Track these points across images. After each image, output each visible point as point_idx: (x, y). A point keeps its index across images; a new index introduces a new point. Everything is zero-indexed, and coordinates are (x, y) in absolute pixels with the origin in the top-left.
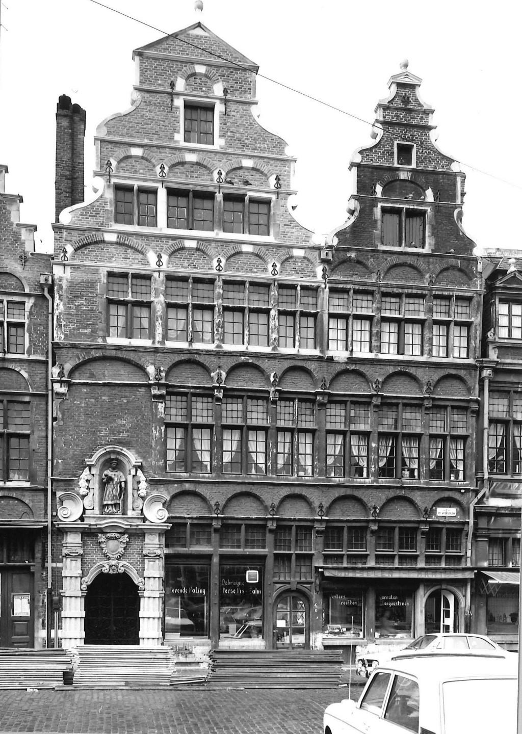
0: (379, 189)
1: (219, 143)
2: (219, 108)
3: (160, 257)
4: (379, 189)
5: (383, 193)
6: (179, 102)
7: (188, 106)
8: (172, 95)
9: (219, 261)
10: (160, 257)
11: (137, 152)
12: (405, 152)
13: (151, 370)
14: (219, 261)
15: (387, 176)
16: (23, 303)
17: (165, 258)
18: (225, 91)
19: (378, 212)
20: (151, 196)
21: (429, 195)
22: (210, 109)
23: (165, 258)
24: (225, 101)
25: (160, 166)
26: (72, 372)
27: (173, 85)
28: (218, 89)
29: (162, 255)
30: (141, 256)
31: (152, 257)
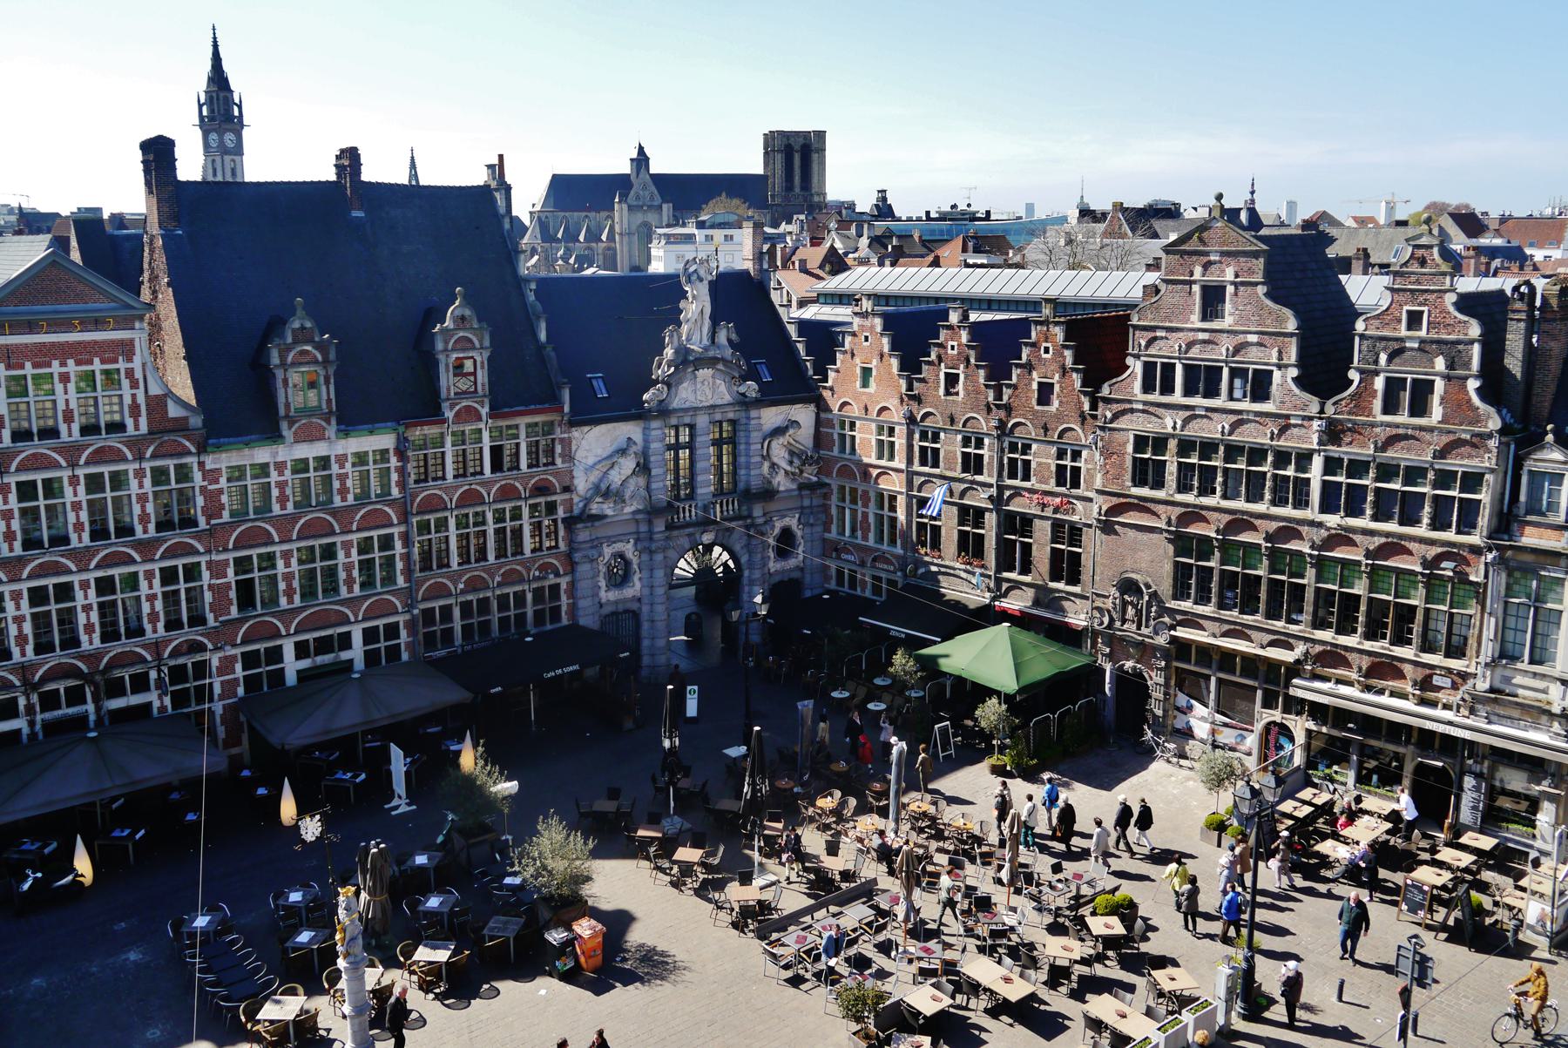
0: (1383, 358)
4: (1383, 358)
5: (1390, 360)
9: (1223, 427)
10: (1175, 423)
12: (1414, 320)
13: (1163, 517)
14: (1223, 427)
15: (1396, 346)
17: (1179, 423)
18: (1237, 276)
19: (1379, 383)
21: (1440, 364)
24: (1235, 284)
26: (1107, 512)
28: (1229, 275)
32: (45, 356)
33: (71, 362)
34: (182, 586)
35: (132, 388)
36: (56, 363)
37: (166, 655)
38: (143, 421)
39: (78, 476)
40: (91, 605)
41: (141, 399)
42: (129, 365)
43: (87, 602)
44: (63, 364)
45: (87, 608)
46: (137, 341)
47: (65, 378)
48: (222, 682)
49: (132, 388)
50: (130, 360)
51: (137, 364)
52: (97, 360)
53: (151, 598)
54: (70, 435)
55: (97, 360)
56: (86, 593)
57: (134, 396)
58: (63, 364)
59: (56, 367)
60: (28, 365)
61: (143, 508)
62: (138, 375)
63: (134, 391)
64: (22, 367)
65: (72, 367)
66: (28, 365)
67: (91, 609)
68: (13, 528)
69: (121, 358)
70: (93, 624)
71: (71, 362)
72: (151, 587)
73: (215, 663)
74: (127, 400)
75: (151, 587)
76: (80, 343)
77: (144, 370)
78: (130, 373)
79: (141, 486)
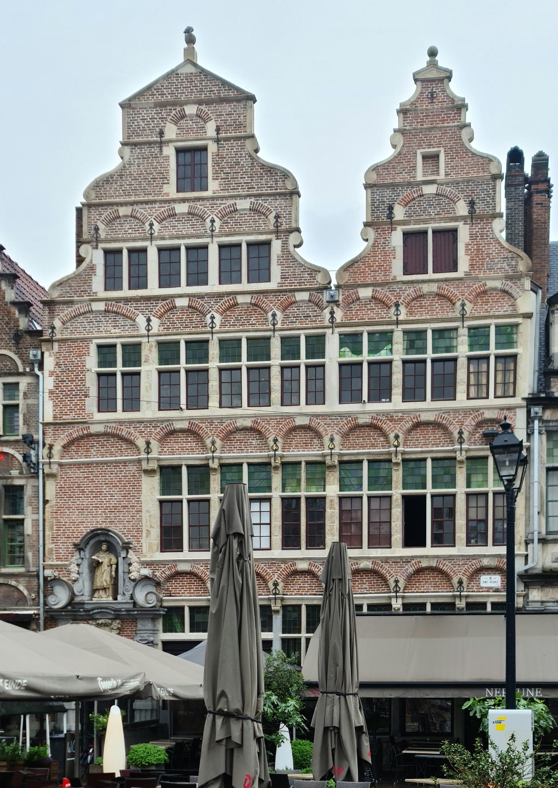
1: (213, 186)
2: (212, 148)
3: (149, 320)
6: (170, 151)
7: (179, 151)
8: (161, 144)
10: (149, 320)
11: (123, 211)
16: (17, 384)
17: (155, 322)
18: (218, 130)
20: (142, 255)
22: (204, 149)
23: (155, 322)
24: (217, 141)
25: (148, 222)
27: (161, 133)
29: (152, 318)
30: (129, 322)
31: (141, 320)
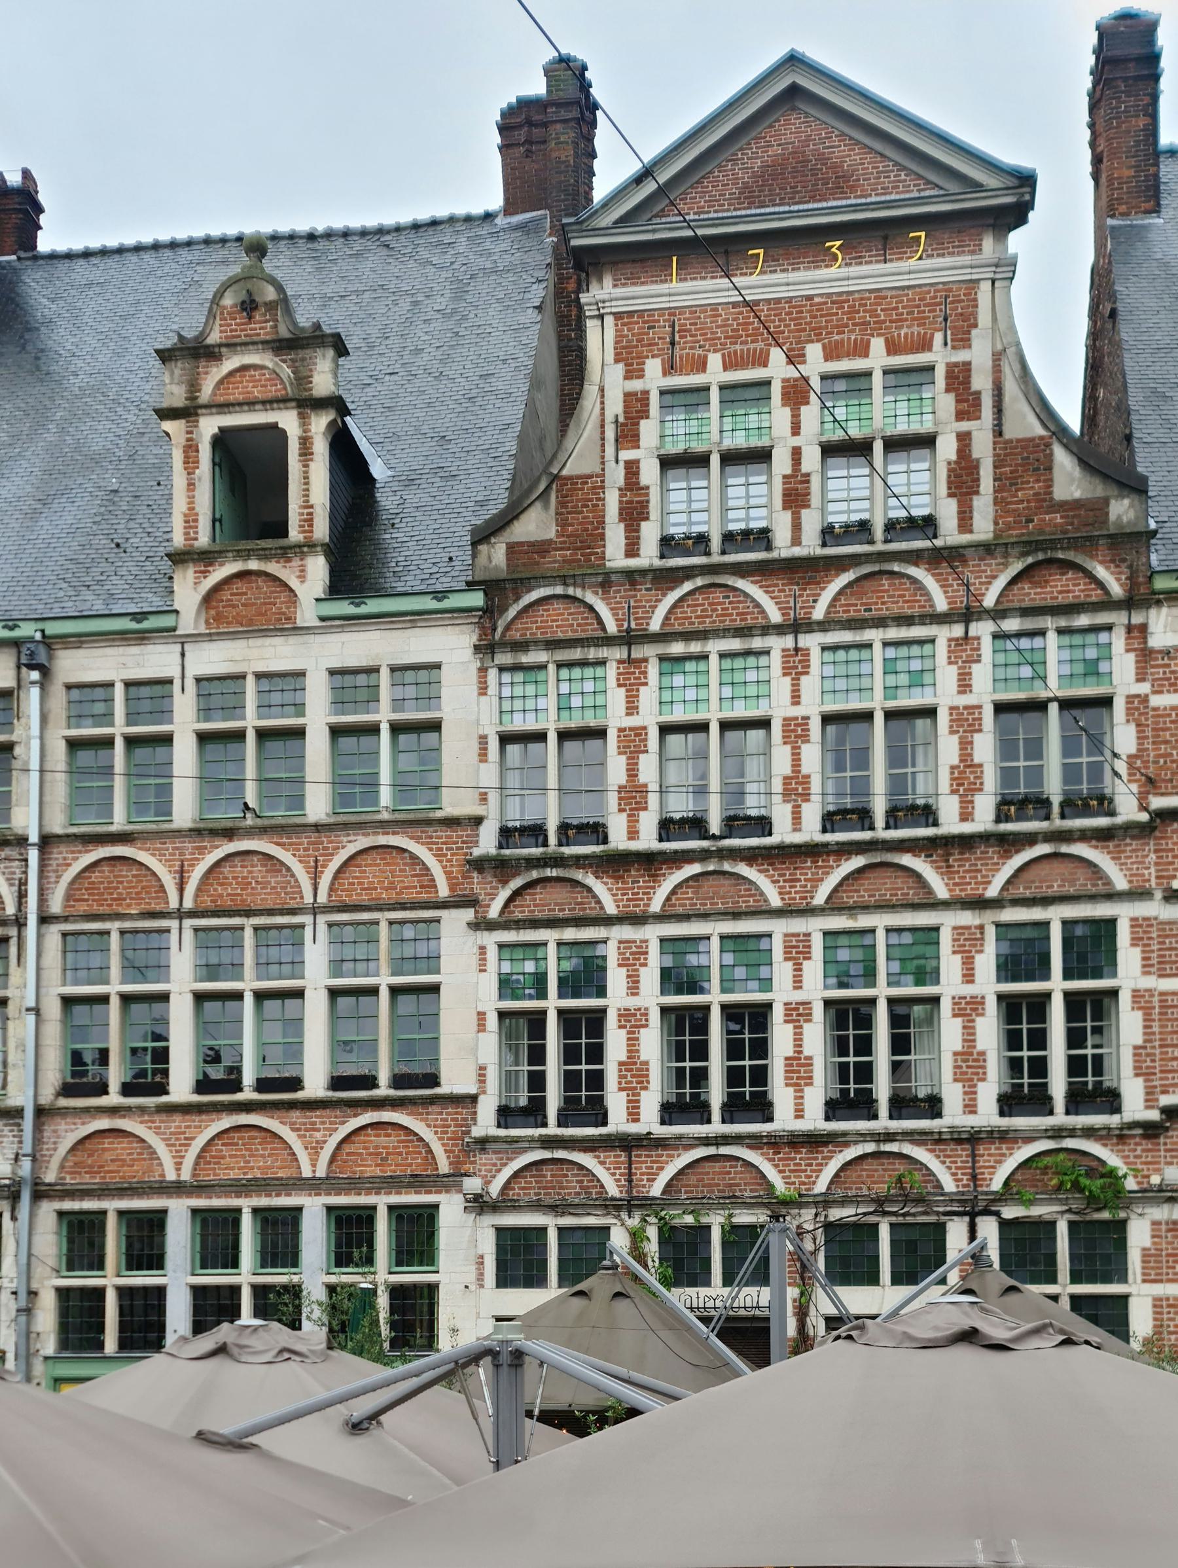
32: (755, 338)
33: (814, 351)
34: (1057, 984)
35: (960, 416)
36: (777, 356)
37: (997, 1185)
38: (983, 506)
39: (806, 652)
40: (807, 1004)
41: (983, 448)
42: (961, 356)
43: (798, 996)
44: (796, 358)
45: (798, 1013)
46: (985, 286)
47: (796, 394)
48: (1158, 1303)
49: (960, 416)
50: (962, 340)
51: (979, 354)
52: (878, 345)
53: (969, 1008)
54: (796, 540)
55: (878, 345)
56: (798, 969)
57: (964, 439)
58: (796, 358)
59: (777, 368)
60: (715, 361)
61: (966, 746)
62: (981, 382)
63: (965, 426)
64: (701, 366)
65: (815, 363)
66: (715, 361)
67: (808, 1017)
68: (643, 778)
69: (938, 338)
70: (809, 1062)
71: (814, 351)
72: (969, 977)
73: (1139, 1235)
74: (947, 448)
75: (969, 977)
76: (838, 300)
77: (997, 370)
78: (959, 378)
79: (964, 685)
